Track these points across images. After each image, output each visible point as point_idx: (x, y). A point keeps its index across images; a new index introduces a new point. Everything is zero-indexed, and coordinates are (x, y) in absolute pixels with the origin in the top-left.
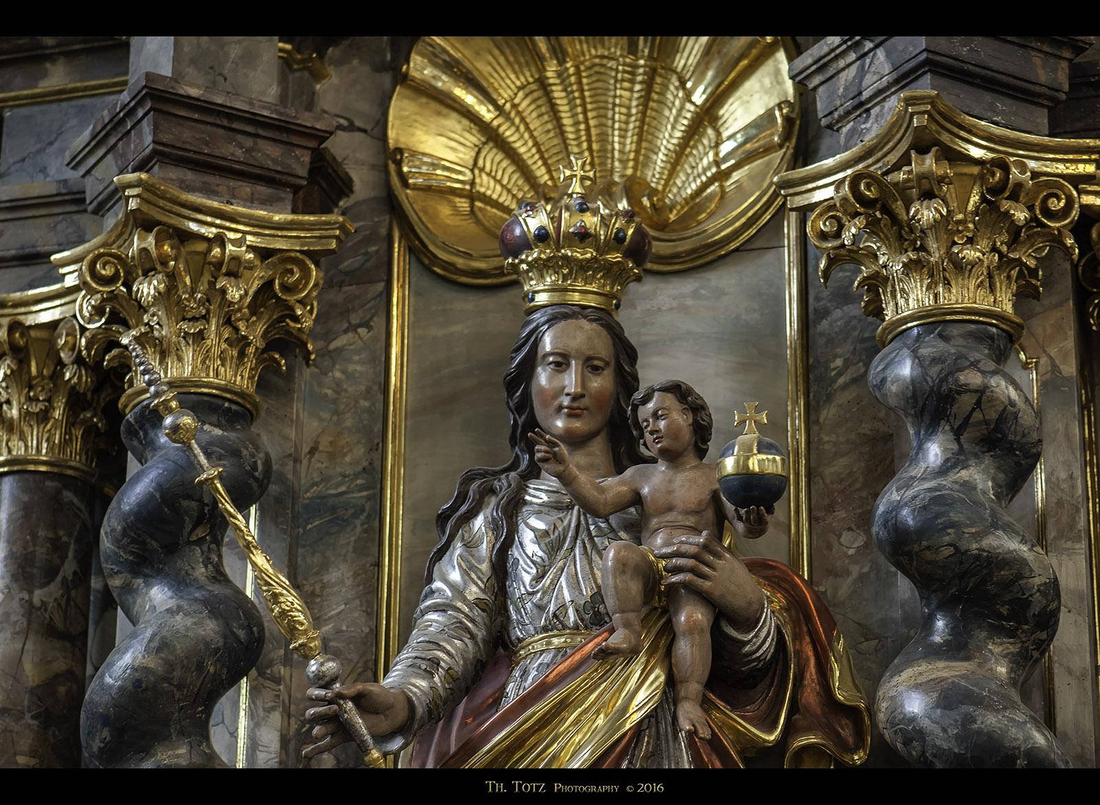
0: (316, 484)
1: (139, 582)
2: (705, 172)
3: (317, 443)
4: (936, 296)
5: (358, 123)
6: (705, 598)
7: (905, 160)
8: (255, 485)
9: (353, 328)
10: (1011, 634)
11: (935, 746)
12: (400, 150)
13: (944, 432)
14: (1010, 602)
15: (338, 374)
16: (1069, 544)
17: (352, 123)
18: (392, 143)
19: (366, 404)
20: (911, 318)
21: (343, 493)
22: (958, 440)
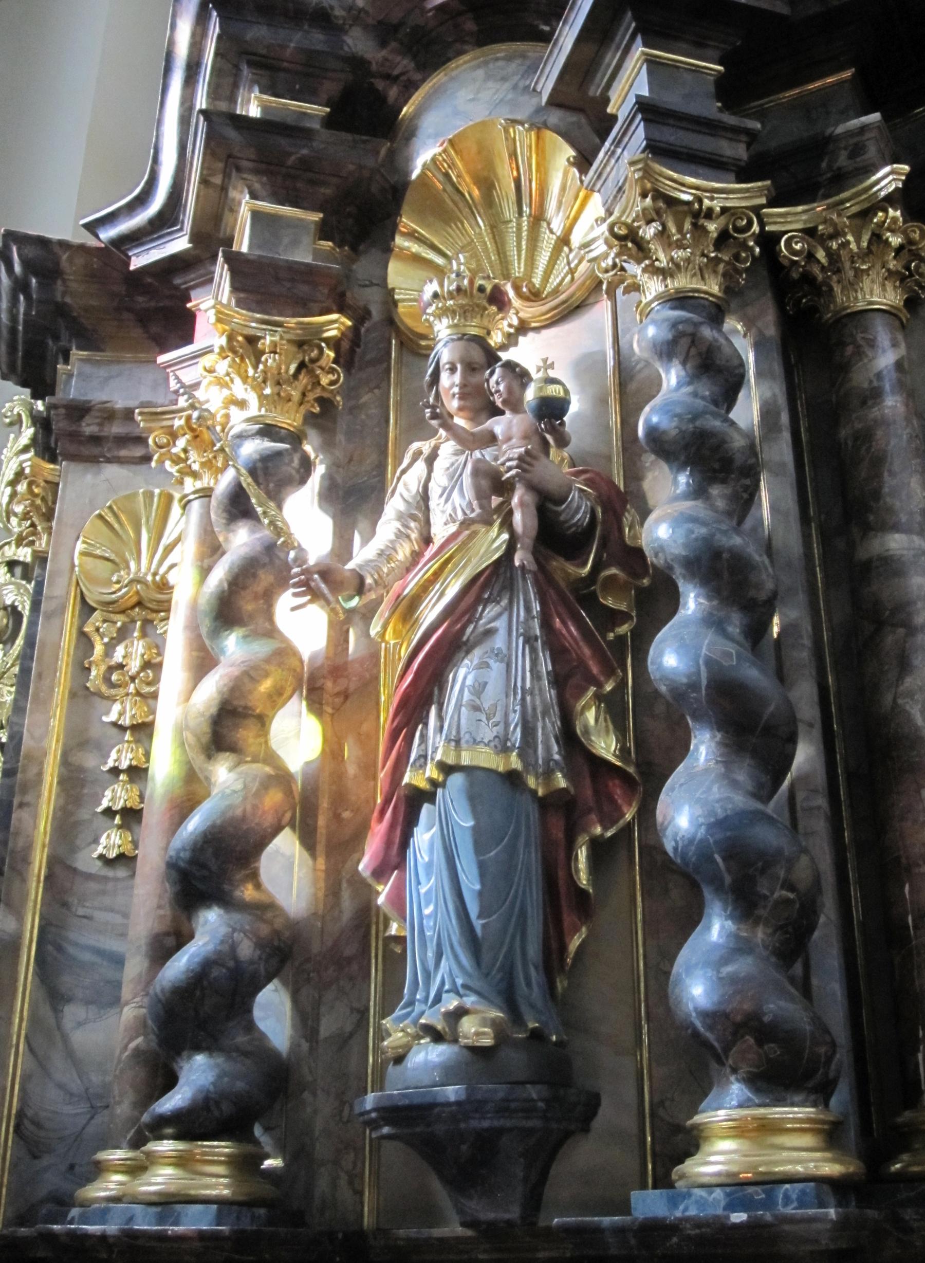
2: (562, 269)
5: (374, 281)
10: (724, 481)
11: (672, 554)
12: (393, 289)
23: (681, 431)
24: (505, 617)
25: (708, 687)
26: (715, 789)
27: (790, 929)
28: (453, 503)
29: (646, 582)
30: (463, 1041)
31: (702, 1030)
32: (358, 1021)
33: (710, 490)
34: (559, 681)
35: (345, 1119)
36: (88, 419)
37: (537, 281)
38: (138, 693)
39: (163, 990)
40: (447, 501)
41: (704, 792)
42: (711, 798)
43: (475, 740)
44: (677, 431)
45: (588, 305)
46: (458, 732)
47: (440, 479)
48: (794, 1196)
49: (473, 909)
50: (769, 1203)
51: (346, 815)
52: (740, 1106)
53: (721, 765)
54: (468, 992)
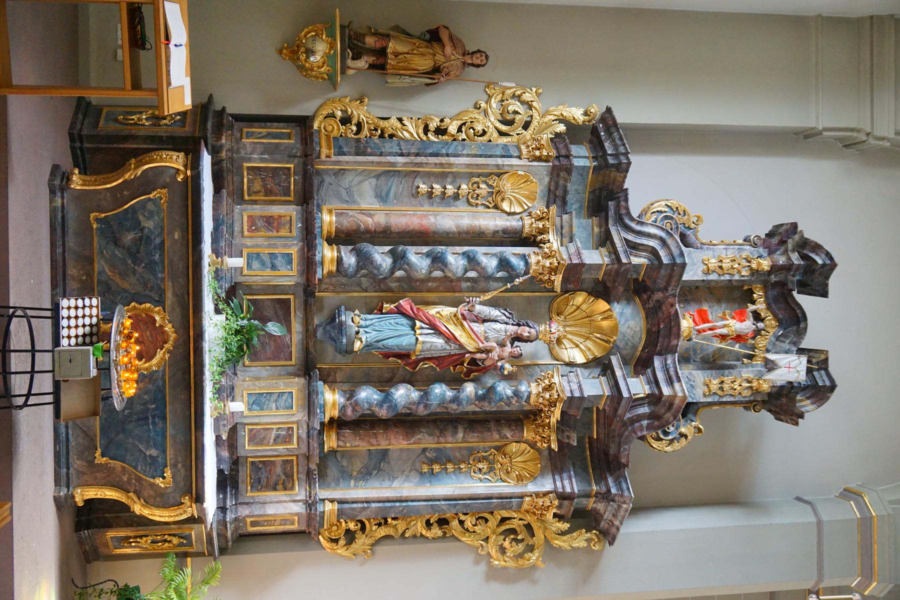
7: (557, 391)
36: (565, 173)
38: (469, 193)
47: (498, 326)
49: (384, 342)
51: (418, 283)
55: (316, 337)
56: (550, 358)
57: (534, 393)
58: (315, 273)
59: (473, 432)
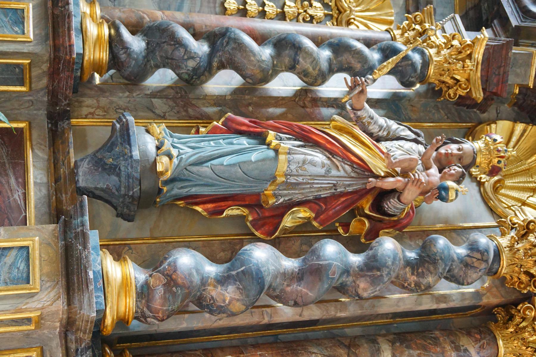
0: (404, 107)
1: (376, 51)
3: (415, 107)
4: (505, 248)
5: (499, 115)
6: (406, 184)
8: (407, 78)
9: (446, 115)
11: (378, 249)
12: (496, 123)
13: (467, 252)
14: (423, 272)
15: (433, 111)
16: (435, 301)
17: (499, 113)
18: (497, 122)
19: (427, 118)
20: (497, 241)
21: (403, 113)
22: (465, 256)
23: (436, 253)
24: (346, 175)
25: (319, 264)
26: (273, 268)
27: (212, 302)
28: (396, 151)
29: (363, 240)
30: (158, 158)
31: (168, 261)
32: (160, 116)
33: (408, 267)
34: (318, 199)
35: (117, 110)
37: (503, 191)
38: (299, 14)
39: (173, 27)
40: (397, 148)
41: (272, 263)
42: (269, 266)
43: (290, 161)
44: (436, 252)
45: (493, 214)
46: (293, 154)
47: (408, 145)
48: (99, 300)
50: (97, 289)
51: (250, 108)
52: (135, 278)
53: (284, 271)
54: (179, 160)
55: (76, 182)
56: (492, 219)
57: (504, 245)
58: (71, 46)
59: (408, 347)
